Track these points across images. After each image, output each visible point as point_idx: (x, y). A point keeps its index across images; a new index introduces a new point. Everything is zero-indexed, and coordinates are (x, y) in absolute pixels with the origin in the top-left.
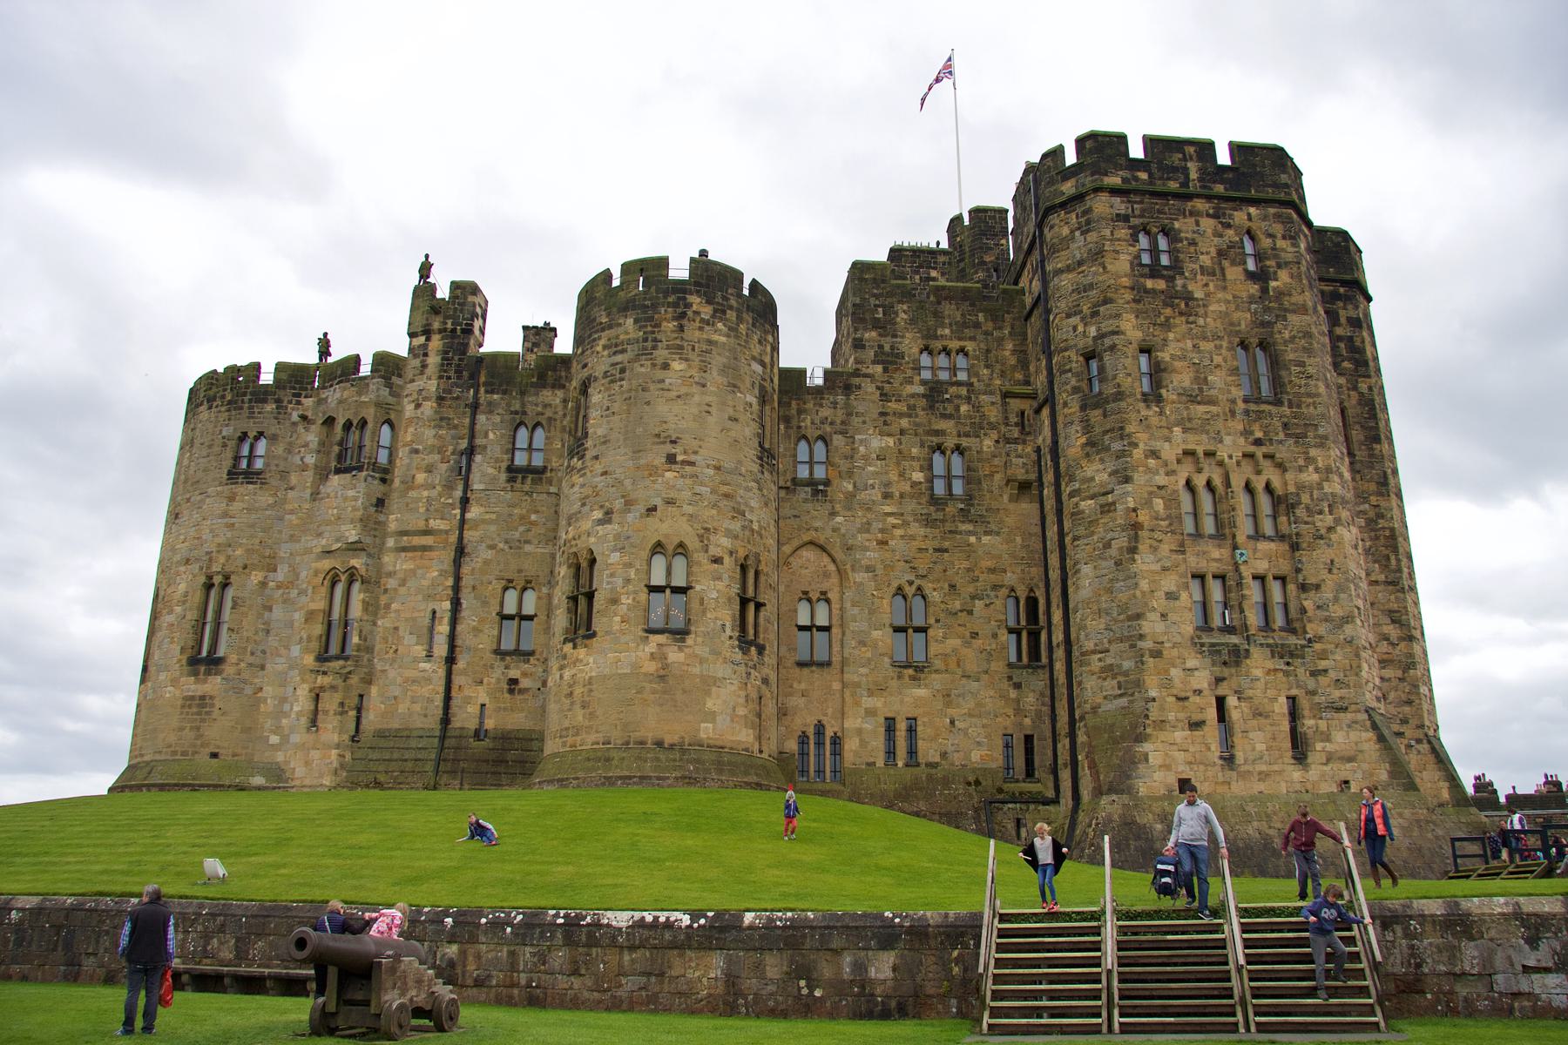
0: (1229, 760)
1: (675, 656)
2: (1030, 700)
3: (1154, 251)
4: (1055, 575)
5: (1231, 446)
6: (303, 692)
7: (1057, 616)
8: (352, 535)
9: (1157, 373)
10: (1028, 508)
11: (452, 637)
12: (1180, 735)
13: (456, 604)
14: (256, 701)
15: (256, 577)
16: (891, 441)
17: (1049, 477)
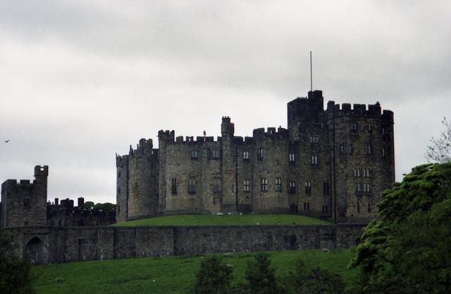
0: (359, 212)
1: (280, 195)
2: (327, 201)
3: (354, 127)
4: (333, 180)
5: (363, 162)
6: (211, 198)
7: (333, 187)
8: (218, 171)
10: (328, 167)
11: (237, 189)
12: (352, 208)
13: (237, 184)
14: (202, 199)
15: (199, 178)
16: (305, 154)
17: (332, 163)
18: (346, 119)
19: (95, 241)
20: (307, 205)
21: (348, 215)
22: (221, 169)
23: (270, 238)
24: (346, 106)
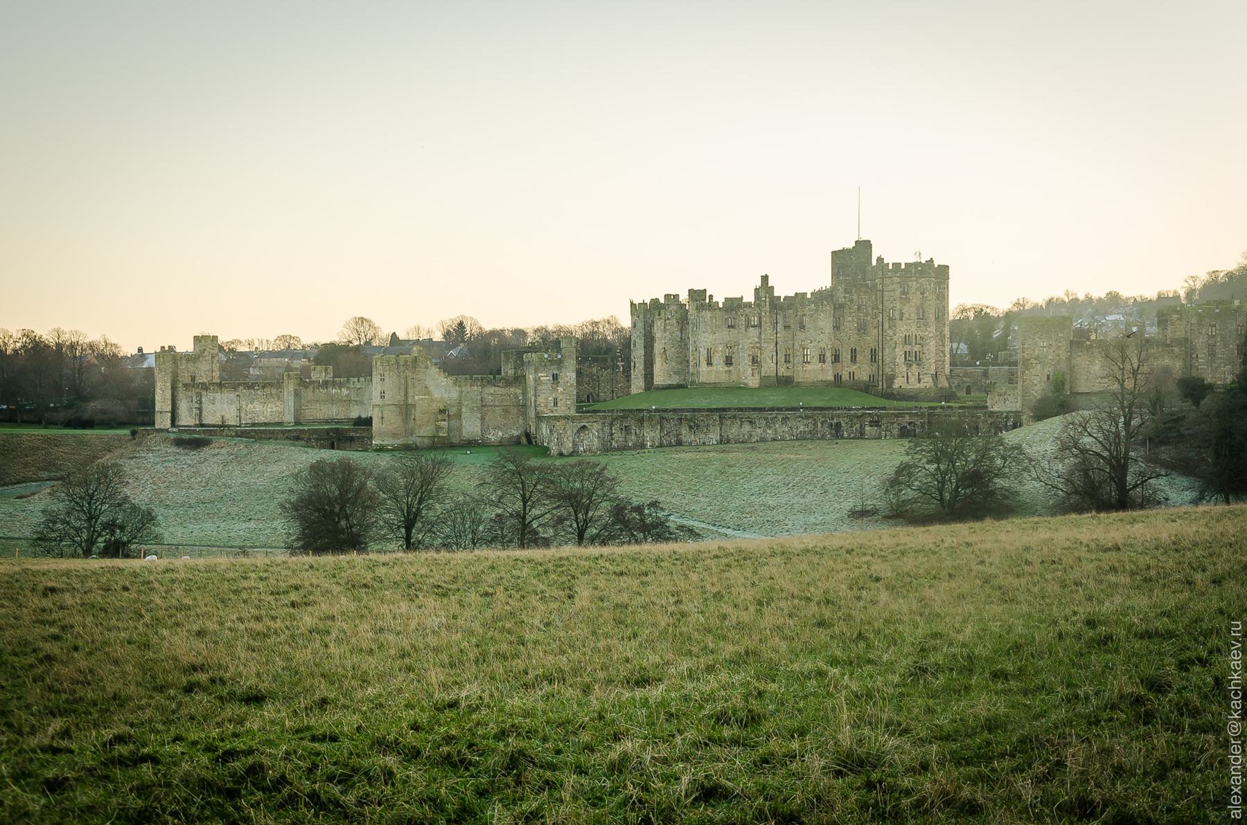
5: (914, 328)
9: (902, 315)
18: (896, 280)
21: (896, 386)
22: (760, 338)
23: (815, 424)
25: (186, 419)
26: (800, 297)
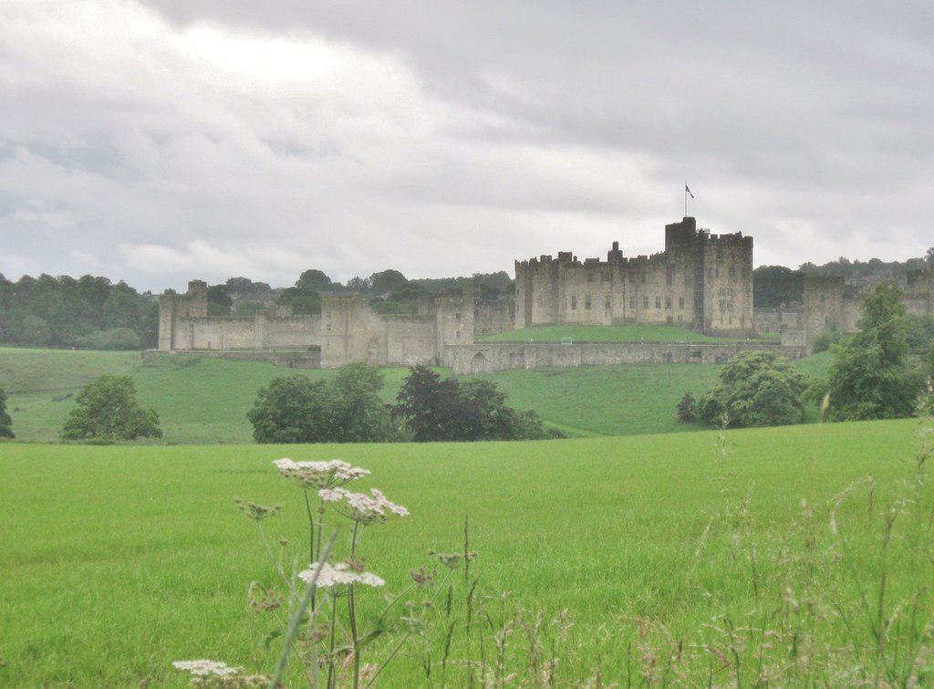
5: (726, 283)
8: (609, 290)
19: (522, 355)
20: (680, 318)
23: (653, 354)
24: (714, 237)
25: (182, 343)
26: (642, 259)
